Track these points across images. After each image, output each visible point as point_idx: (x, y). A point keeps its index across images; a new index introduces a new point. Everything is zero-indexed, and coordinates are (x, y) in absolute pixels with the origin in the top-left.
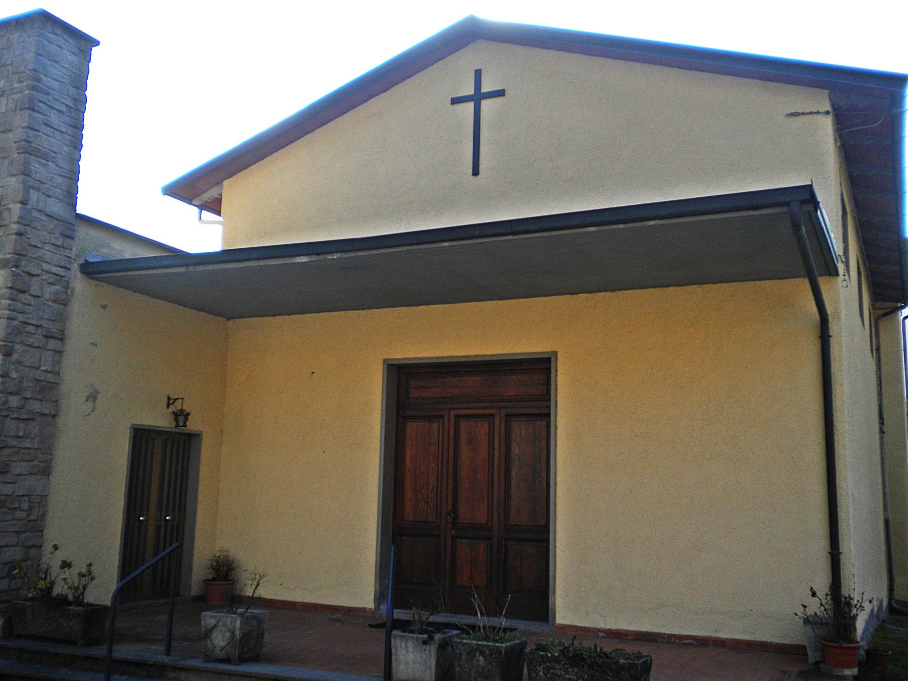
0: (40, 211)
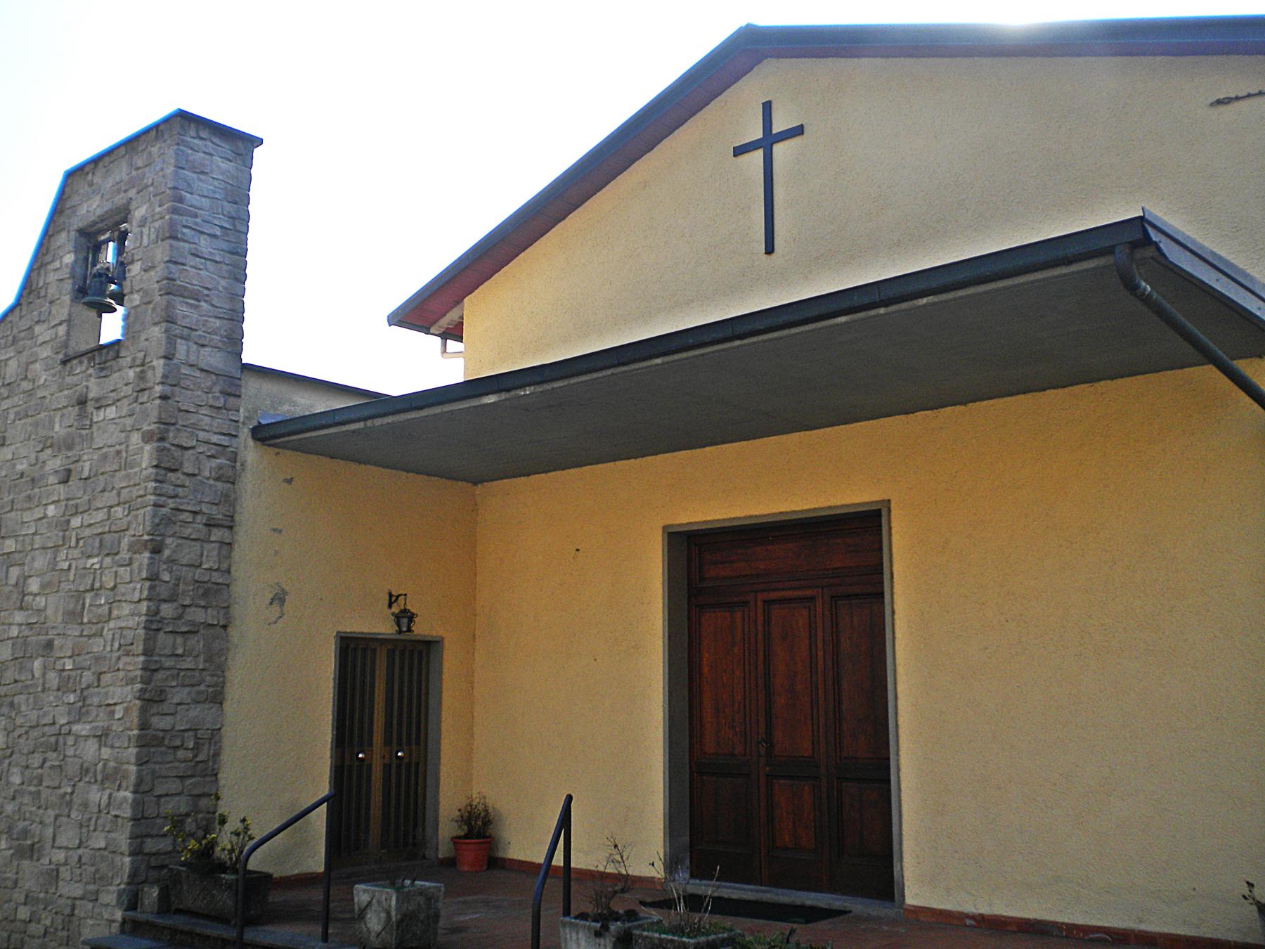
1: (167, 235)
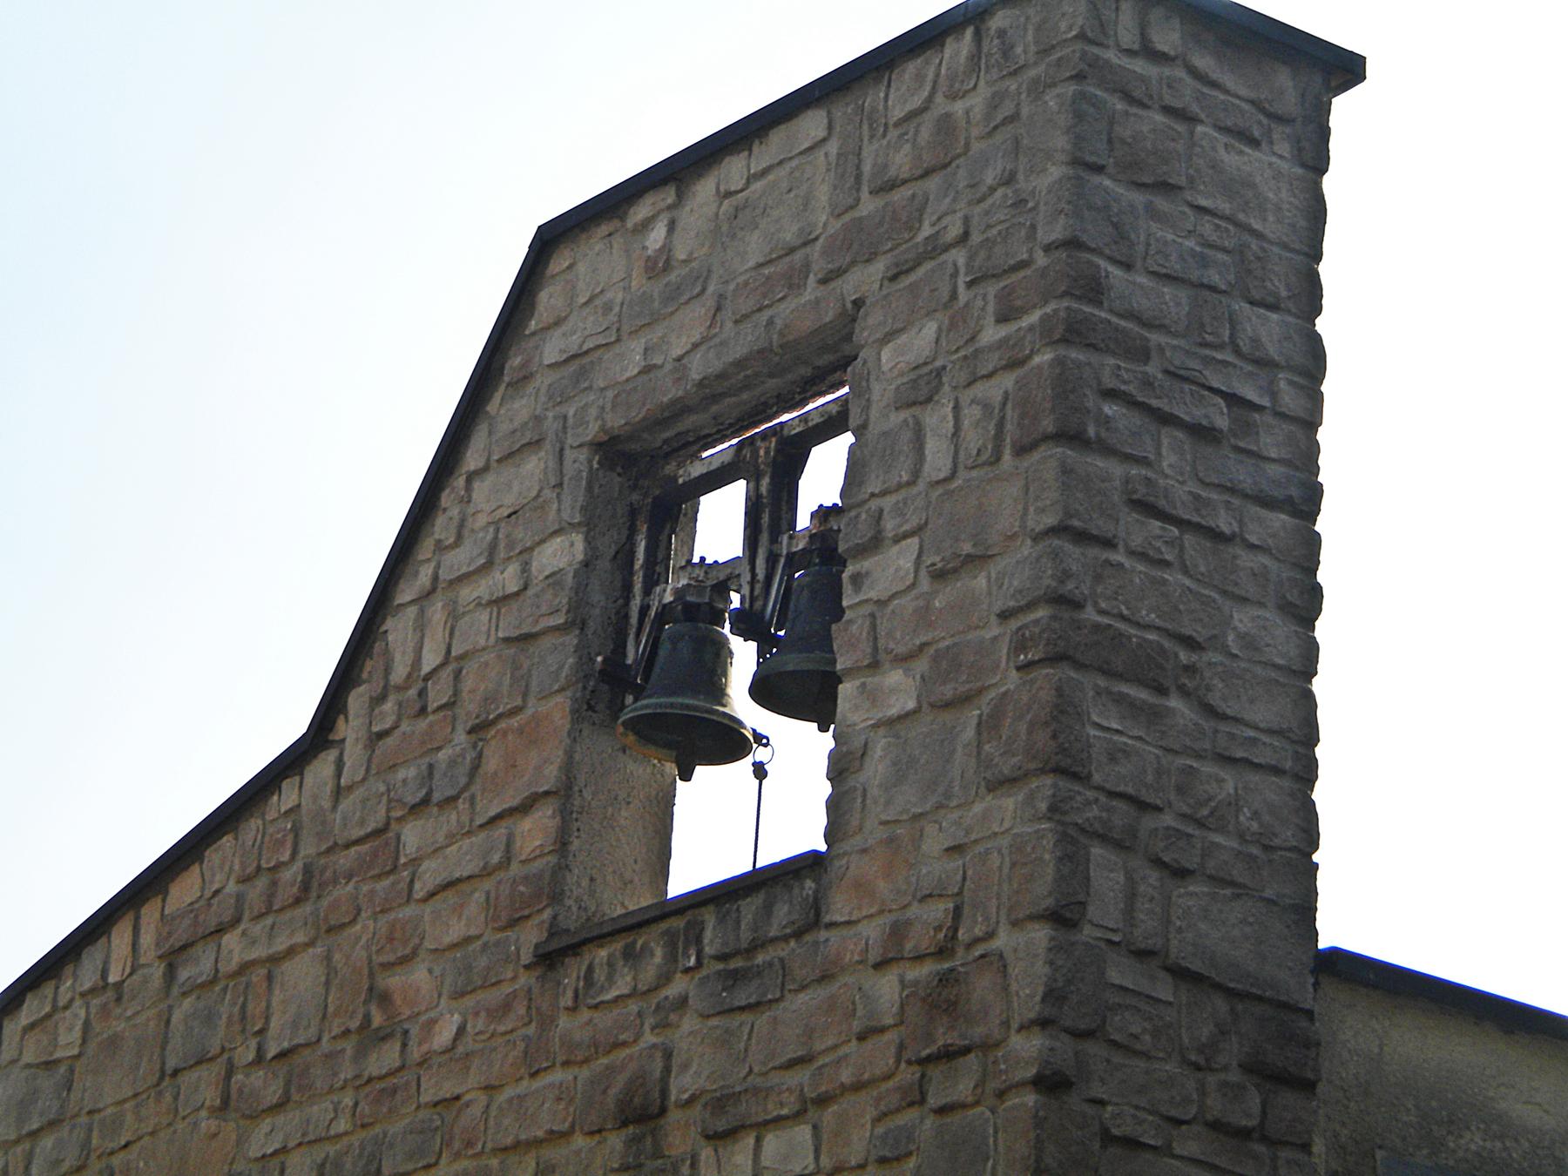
0: (1143, 954)
1: (1048, 424)
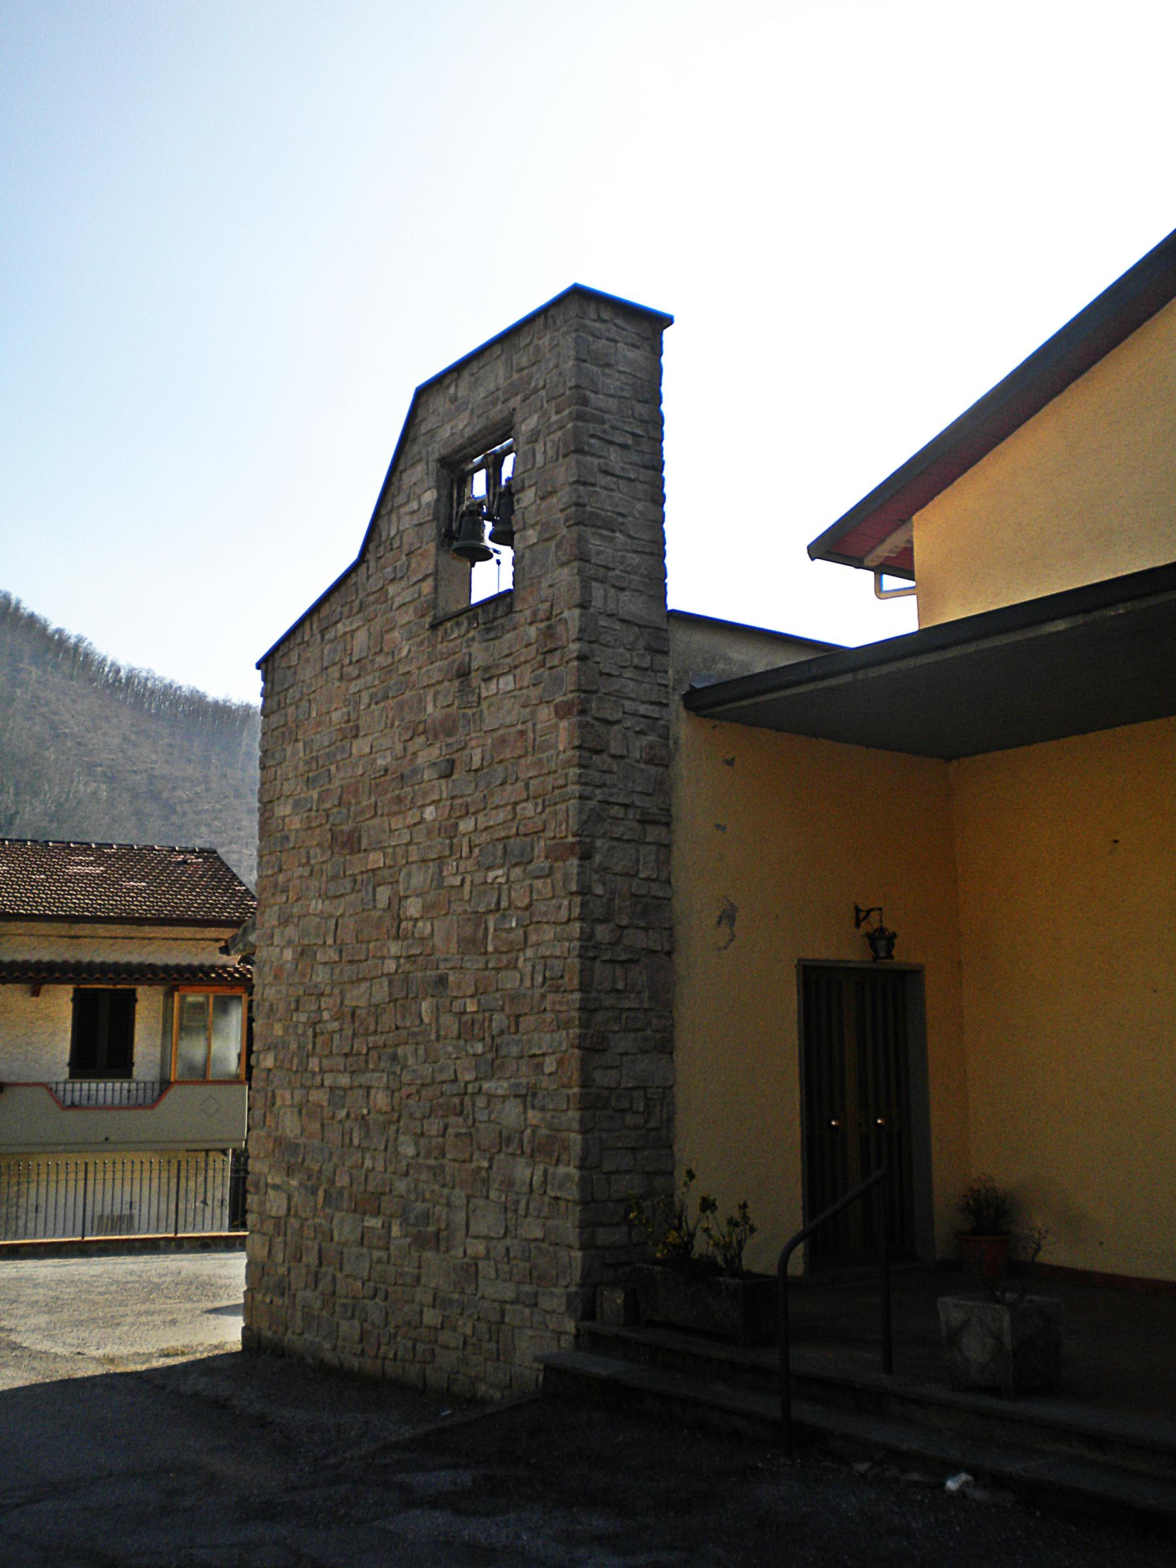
0: (610, 616)
1: (572, 448)
